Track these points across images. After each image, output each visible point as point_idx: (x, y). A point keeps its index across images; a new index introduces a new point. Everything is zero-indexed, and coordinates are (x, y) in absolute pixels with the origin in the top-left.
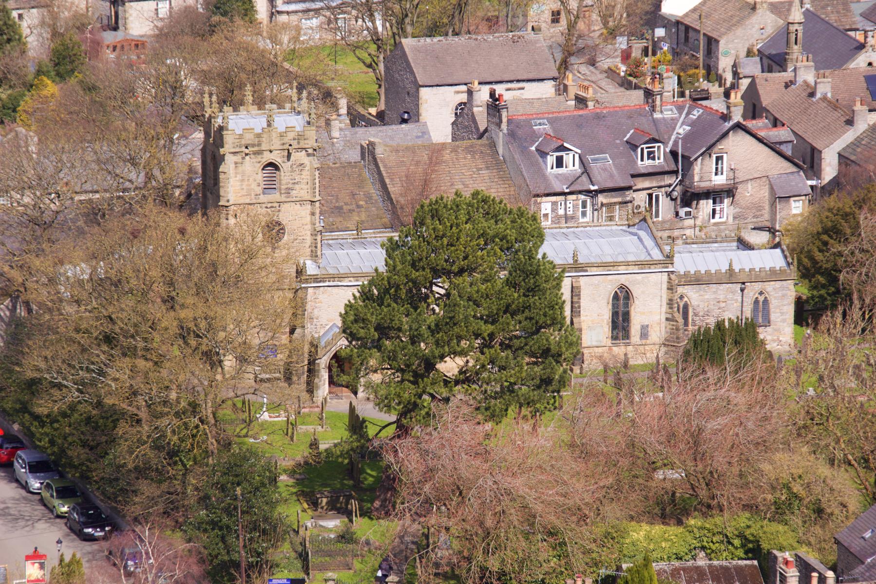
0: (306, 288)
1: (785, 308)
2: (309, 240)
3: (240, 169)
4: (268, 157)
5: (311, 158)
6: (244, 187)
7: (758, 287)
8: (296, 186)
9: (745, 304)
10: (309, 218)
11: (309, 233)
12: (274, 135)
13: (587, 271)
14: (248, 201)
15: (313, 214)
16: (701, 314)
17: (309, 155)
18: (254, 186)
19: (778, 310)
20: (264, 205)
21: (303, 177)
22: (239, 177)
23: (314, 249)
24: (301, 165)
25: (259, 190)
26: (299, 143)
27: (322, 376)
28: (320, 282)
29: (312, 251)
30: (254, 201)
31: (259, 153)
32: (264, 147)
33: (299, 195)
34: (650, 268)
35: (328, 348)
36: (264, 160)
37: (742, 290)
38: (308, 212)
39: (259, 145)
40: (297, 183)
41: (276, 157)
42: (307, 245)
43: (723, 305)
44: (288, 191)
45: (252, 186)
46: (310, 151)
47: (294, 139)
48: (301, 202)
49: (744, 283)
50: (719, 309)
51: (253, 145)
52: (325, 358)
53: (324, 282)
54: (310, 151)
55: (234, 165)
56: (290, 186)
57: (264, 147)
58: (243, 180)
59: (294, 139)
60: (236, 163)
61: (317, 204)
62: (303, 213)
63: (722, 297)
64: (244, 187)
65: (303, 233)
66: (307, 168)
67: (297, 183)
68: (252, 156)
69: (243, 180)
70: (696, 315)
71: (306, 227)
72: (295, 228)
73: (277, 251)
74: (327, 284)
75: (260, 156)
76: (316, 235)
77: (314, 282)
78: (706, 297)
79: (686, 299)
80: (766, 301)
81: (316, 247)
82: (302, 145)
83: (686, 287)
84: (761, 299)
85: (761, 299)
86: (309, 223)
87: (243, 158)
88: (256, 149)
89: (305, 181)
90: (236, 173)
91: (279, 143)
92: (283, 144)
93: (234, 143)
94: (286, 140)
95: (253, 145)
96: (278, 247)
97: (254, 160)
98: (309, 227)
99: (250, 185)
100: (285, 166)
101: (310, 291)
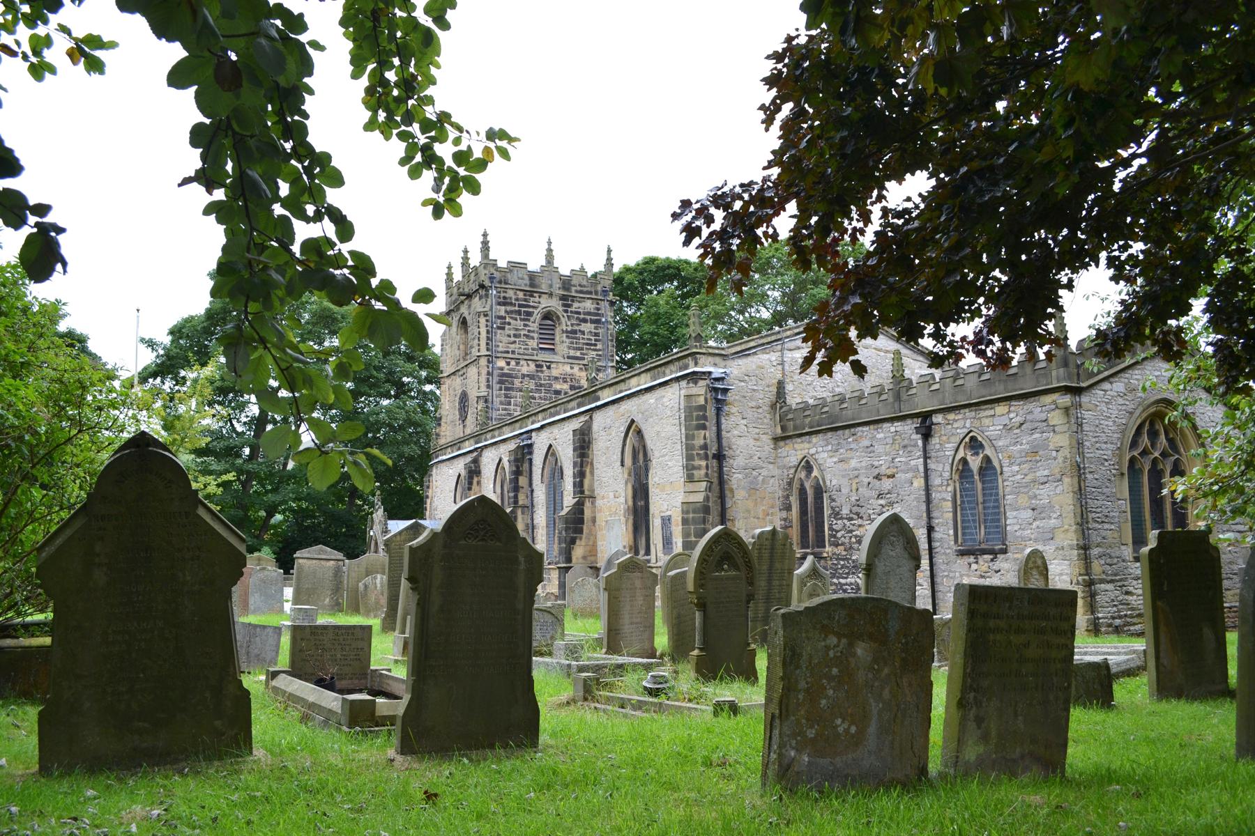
1: (1045, 494)
7: (960, 425)
9: (936, 481)
13: (598, 399)
16: (845, 511)
19: (1023, 500)
34: (664, 375)
37: (927, 434)
43: (887, 484)
49: (926, 416)
50: (880, 496)
63: (883, 464)
70: (836, 514)
78: (853, 463)
79: (815, 473)
80: (987, 467)
83: (815, 439)
84: (975, 463)
85: (975, 463)
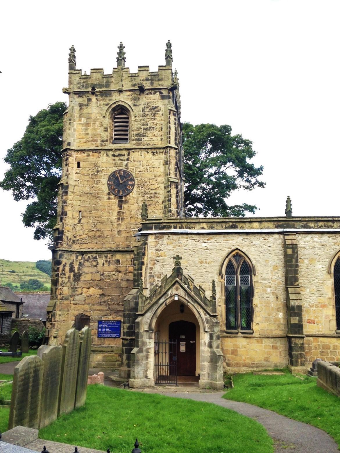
0: (147, 235)
2: (162, 194)
3: (85, 111)
4: (116, 97)
5: (166, 101)
6: (89, 131)
8: (149, 133)
10: (162, 169)
11: (162, 186)
12: (125, 75)
14: (93, 147)
15: (167, 163)
17: (163, 97)
18: (100, 131)
20: (111, 153)
21: (156, 122)
22: (84, 120)
23: (167, 203)
24: (154, 108)
25: (105, 135)
26: (152, 84)
27: (144, 344)
28: (163, 228)
29: (165, 207)
30: (100, 148)
31: (108, 94)
32: (113, 87)
33: (152, 143)
35: (154, 300)
36: (111, 103)
38: (162, 162)
39: (108, 85)
40: (150, 129)
41: (125, 99)
42: (160, 201)
44: (139, 137)
45: (99, 131)
46: (165, 93)
47: (147, 80)
48: (154, 150)
51: (101, 86)
52: (149, 315)
53: (169, 228)
54: (165, 93)
55: (78, 108)
56: (141, 131)
57: (113, 87)
58: (88, 124)
59: (147, 80)
60: (81, 105)
61: (173, 152)
62: (156, 164)
64: (89, 131)
65: (156, 186)
66: (161, 113)
67: (150, 129)
68: (99, 98)
69: (88, 124)
71: (159, 179)
72: (146, 179)
73: (125, 206)
74: (173, 230)
75: (108, 98)
76: (170, 186)
77: (156, 228)
81: (169, 200)
82: (155, 86)
86: (162, 174)
87: (90, 100)
88: (104, 89)
89: (159, 126)
90: (81, 116)
91: (130, 84)
92: (134, 85)
93: (78, 83)
94: (138, 81)
95: (101, 86)
96: (126, 202)
97: (102, 103)
98: (162, 179)
99: (95, 130)
100: (136, 112)
101: (151, 240)
